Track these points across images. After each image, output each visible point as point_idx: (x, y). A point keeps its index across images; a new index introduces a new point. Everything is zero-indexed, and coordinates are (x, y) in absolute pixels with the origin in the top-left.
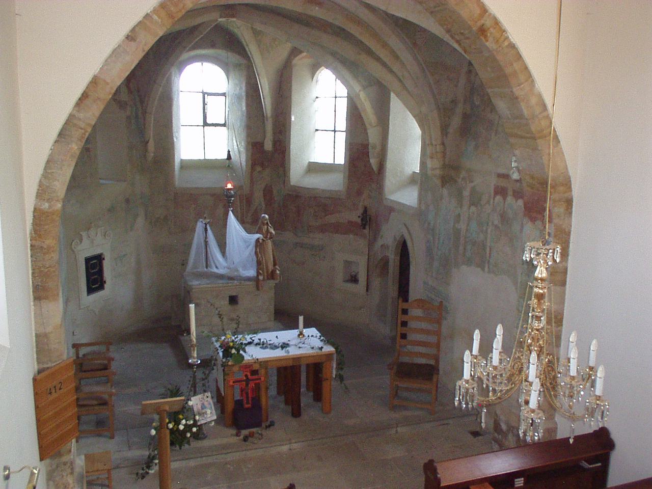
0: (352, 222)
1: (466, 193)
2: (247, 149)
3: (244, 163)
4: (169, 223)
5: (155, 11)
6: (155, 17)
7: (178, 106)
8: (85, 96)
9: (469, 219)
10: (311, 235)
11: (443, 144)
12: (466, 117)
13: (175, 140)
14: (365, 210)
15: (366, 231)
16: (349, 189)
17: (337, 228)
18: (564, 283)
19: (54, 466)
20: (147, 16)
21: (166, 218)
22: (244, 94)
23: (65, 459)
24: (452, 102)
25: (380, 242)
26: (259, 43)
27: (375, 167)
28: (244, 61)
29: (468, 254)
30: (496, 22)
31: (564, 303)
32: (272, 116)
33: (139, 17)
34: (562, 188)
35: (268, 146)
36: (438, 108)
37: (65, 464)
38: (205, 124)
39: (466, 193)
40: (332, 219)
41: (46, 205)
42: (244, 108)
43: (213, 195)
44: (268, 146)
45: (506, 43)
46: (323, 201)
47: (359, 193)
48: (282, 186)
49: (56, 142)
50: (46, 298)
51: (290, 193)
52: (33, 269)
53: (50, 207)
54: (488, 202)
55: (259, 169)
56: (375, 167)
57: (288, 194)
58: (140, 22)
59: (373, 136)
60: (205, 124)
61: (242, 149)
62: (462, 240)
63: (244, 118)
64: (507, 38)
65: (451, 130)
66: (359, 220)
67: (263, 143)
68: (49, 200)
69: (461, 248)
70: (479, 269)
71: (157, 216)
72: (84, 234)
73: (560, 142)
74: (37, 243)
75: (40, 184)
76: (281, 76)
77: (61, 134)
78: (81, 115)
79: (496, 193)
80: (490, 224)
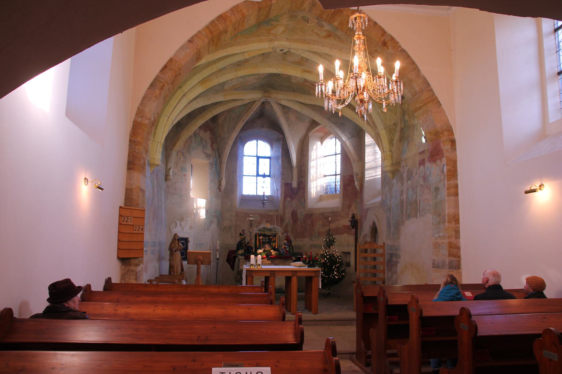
1: (405, 175)
2: (281, 187)
3: (279, 196)
5: (203, 29)
6: (203, 32)
7: (242, 164)
8: (165, 67)
9: (408, 189)
11: (391, 151)
12: (402, 130)
13: (238, 181)
14: (353, 216)
18: (456, 194)
19: (126, 271)
20: (199, 32)
22: (280, 155)
23: (132, 268)
24: (394, 124)
25: (363, 234)
26: (288, 119)
27: (358, 188)
28: (281, 136)
29: (408, 213)
30: (392, 39)
31: (458, 208)
32: (297, 166)
33: (194, 32)
34: (446, 133)
35: (295, 185)
36: (385, 128)
37: (132, 271)
38: (258, 175)
39: (405, 175)
41: (140, 119)
42: (280, 163)
43: (259, 214)
44: (295, 185)
45: (400, 49)
47: (349, 207)
49: (149, 88)
50: (134, 169)
52: (129, 153)
53: (142, 120)
54: (416, 173)
55: (289, 199)
58: (196, 35)
59: (356, 169)
60: (258, 175)
61: (279, 188)
62: (405, 205)
63: (281, 169)
64: (400, 46)
65: (395, 142)
66: (349, 224)
67: (291, 184)
68: (142, 117)
69: (405, 211)
72: (178, 224)
73: (440, 105)
74: (132, 139)
75: (139, 108)
76: (303, 142)
77: (152, 85)
78: (162, 76)
79: (420, 165)
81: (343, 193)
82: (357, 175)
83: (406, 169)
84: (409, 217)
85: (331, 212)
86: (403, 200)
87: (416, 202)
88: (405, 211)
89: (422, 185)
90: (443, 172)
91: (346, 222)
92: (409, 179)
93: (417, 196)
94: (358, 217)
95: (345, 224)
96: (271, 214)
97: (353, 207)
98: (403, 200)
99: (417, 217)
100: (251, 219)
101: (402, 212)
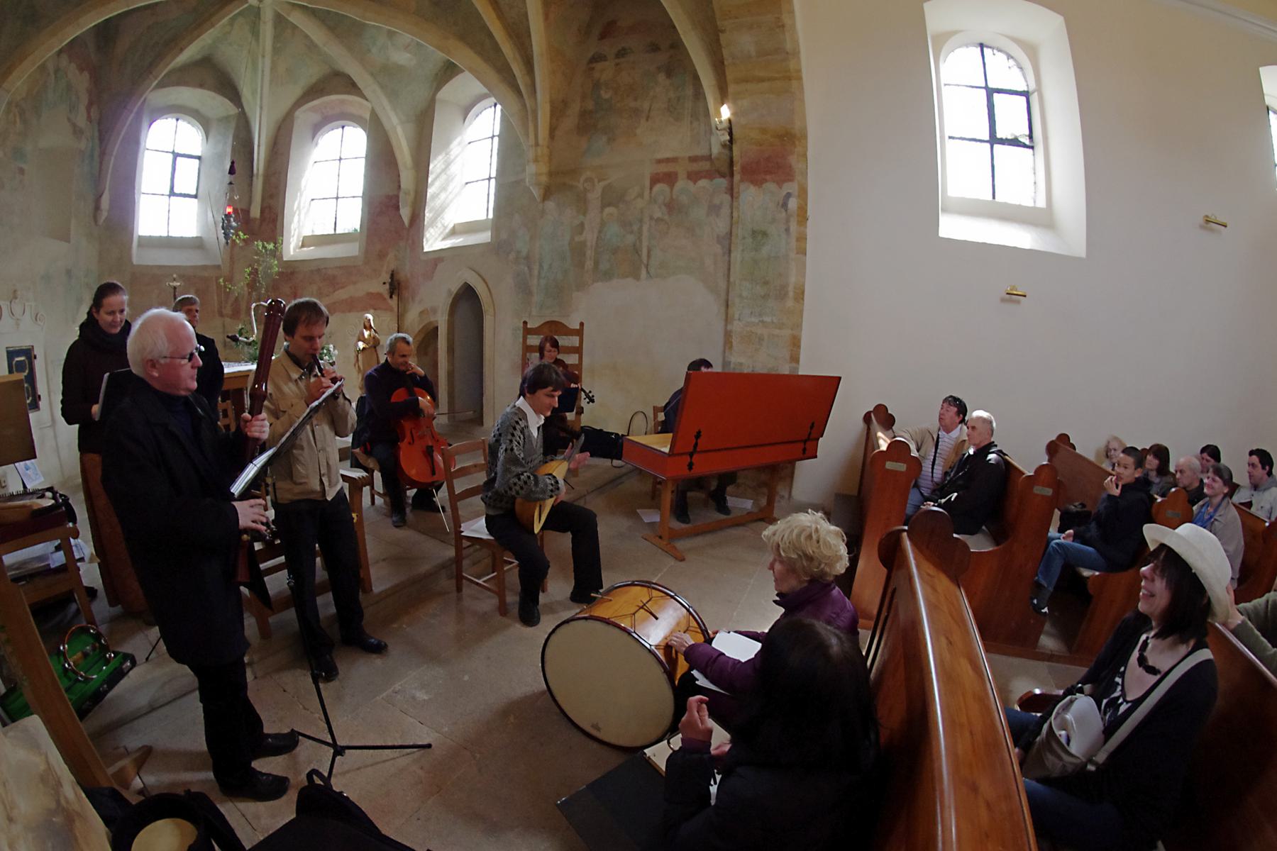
9: (603, 224)
16: (367, 252)
29: (604, 266)
39: (595, 196)
47: (382, 256)
54: (641, 195)
56: (406, 221)
62: (590, 253)
66: (384, 290)
69: (589, 264)
70: (630, 280)
79: (655, 180)
80: (646, 219)
81: (369, 229)
82: (407, 193)
83: (599, 187)
84: (608, 276)
85: (340, 268)
86: (583, 244)
87: (636, 250)
88: (589, 264)
89: (658, 220)
90: (785, 205)
91: (379, 286)
92: (603, 206)
93: (640, 239)
94: (401, 276)
95: (371, 290)
97: (391, 256)
98: (583, 244)
99: (637, 278)
101: (581, 265)
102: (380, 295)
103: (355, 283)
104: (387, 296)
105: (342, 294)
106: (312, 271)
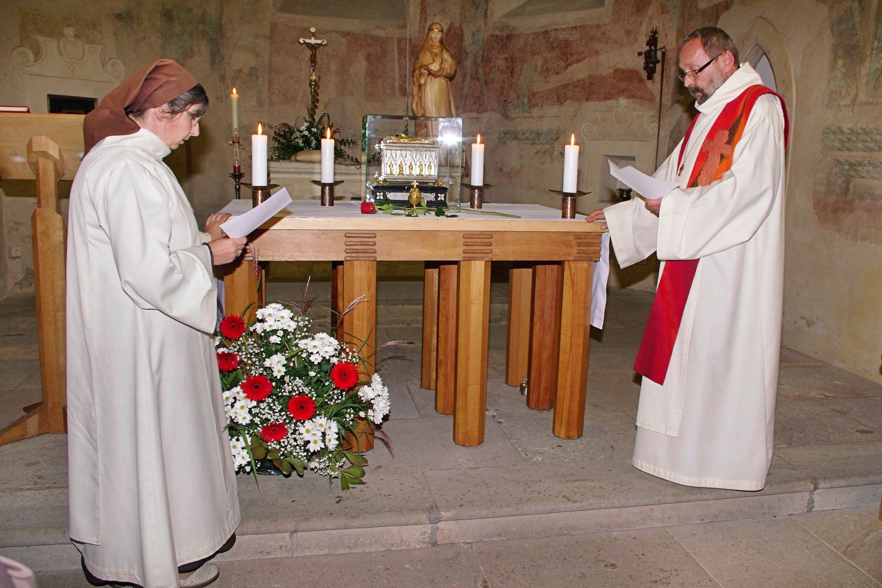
0: (624, 71)
4: (260, 80)
10: (536, 112)
15: (654, 87)
17: (592, 90)
21: (253, 73)
40: (579, 72)
46: (561, 37)
48: (482, 23)
51: (498, 33)
57: (492, 35)
66: (639, 63)
71: (236, 68)
85: (575, 28)
95: (621, 66)
96: (382, 33)
100: (313, 41)
102: (629, 75)
103: (597, 53)
104: (644, 75)
105: (579, 72)
106: (536, 35)
